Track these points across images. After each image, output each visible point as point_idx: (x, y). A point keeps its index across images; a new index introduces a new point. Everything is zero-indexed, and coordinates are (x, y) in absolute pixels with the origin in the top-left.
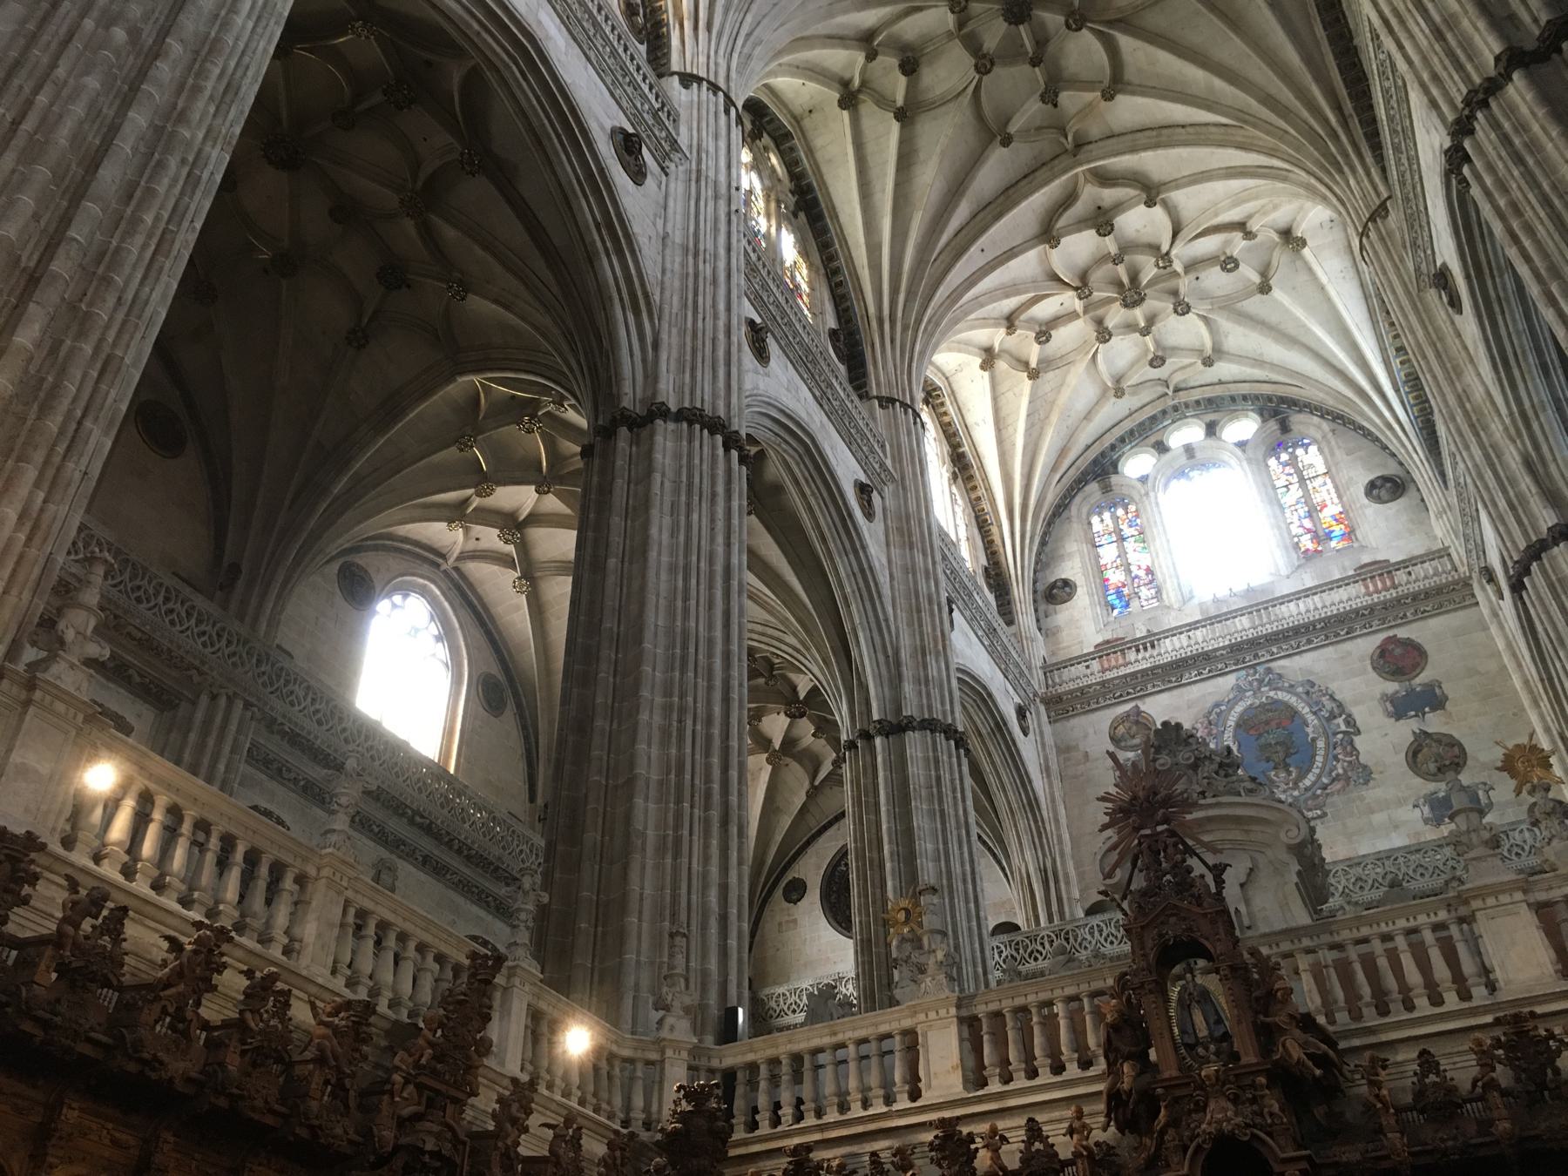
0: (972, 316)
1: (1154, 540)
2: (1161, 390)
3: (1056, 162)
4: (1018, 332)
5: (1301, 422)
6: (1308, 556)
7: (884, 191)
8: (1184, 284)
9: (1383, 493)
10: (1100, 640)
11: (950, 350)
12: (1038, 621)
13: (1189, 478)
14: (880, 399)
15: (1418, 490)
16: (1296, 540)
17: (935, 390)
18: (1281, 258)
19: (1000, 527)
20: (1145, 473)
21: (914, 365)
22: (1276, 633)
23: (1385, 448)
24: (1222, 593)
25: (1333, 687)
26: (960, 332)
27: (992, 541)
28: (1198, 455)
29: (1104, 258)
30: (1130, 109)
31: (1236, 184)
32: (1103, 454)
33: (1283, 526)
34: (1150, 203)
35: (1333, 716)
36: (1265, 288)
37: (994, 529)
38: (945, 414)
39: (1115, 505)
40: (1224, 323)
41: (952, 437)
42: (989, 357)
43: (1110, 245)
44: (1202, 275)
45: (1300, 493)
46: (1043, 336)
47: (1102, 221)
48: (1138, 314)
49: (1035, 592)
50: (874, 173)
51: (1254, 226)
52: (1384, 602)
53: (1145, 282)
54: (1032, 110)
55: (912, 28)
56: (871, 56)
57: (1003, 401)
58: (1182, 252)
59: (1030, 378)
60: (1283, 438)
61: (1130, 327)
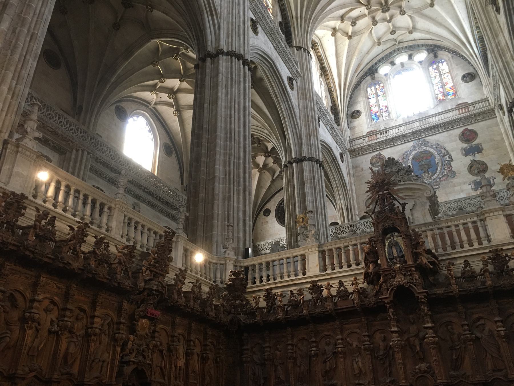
0: (329, 16)
1: (388, 96)
2: (394, 43)
4: (345, 22)
5: (442, 54)
6: (440, 101)
9: (468, 79)
10: (368, 131)
11: (321, 29)
12: (348, 124)
14: (296, 47)
15: (480, 78)
16: (437, 96)
17: (315, 44)
19: (336, 92)
20: (387, 73)
21: (308, 34)
22: (428, 128)
23: (469, 63)
24: (411, 115)
25: (446, 145)
26: (325, 22)
27: (334, 97)
28: (405, 66)
32: (372, 66)
33: (433, 91)
35: (444, 155)
36: (432, 5)
37: (334, 93)
38: (319, 52)
39: (376, 84)
40: (417, 18)
41: (320, 60)
42: (334, 31)
45: (439, 79)
46: (354, 23)
48: (387, 15)
49: (347, 115)
52: (465, 117)
53: (390, 4)
57: (339, 47)
59: (348, 39)
60: (435, 60)
61: (384, 20)
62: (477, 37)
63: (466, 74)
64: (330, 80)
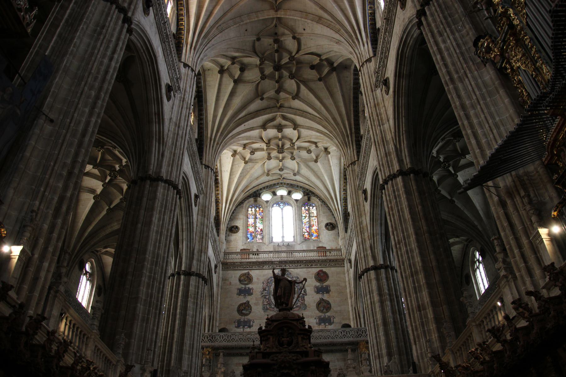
1: (265, 221)
3: (273, 109)
6: (306, 240)
7: (223, 100)
8: (295, 152)
10: (242, 248)
13: (279, 206)
14: (205, 165)
18: (322, 154)
19: (222, 204)
22: (293, 261)
23: (333, 215)
27: (219, 208)
28: (284, 199)
29: (276, 138)
30: (297, 104)
31: (318, 134)
32: (258, 191)
34: (294, 129)
36: (316, 161)
37: (220, 205)
39: (257, 207)
40: (302, 166)
42: (235, 153)
43: (280, 135)
44: (301, 151)
45: (308, 220)
46: (252, 153)
47: (280, 128)
48: (281, 156)
50: (222, 94)
51: (319, 145)
54: (272, 93)
55: (246, 60)
56: (233, 63)
57: (234, 167)
58: (298, 144)
59: (245, 163)
61: (277, 158)
62: (342, 197)
63: (329, 223)
64: (219, 192)
